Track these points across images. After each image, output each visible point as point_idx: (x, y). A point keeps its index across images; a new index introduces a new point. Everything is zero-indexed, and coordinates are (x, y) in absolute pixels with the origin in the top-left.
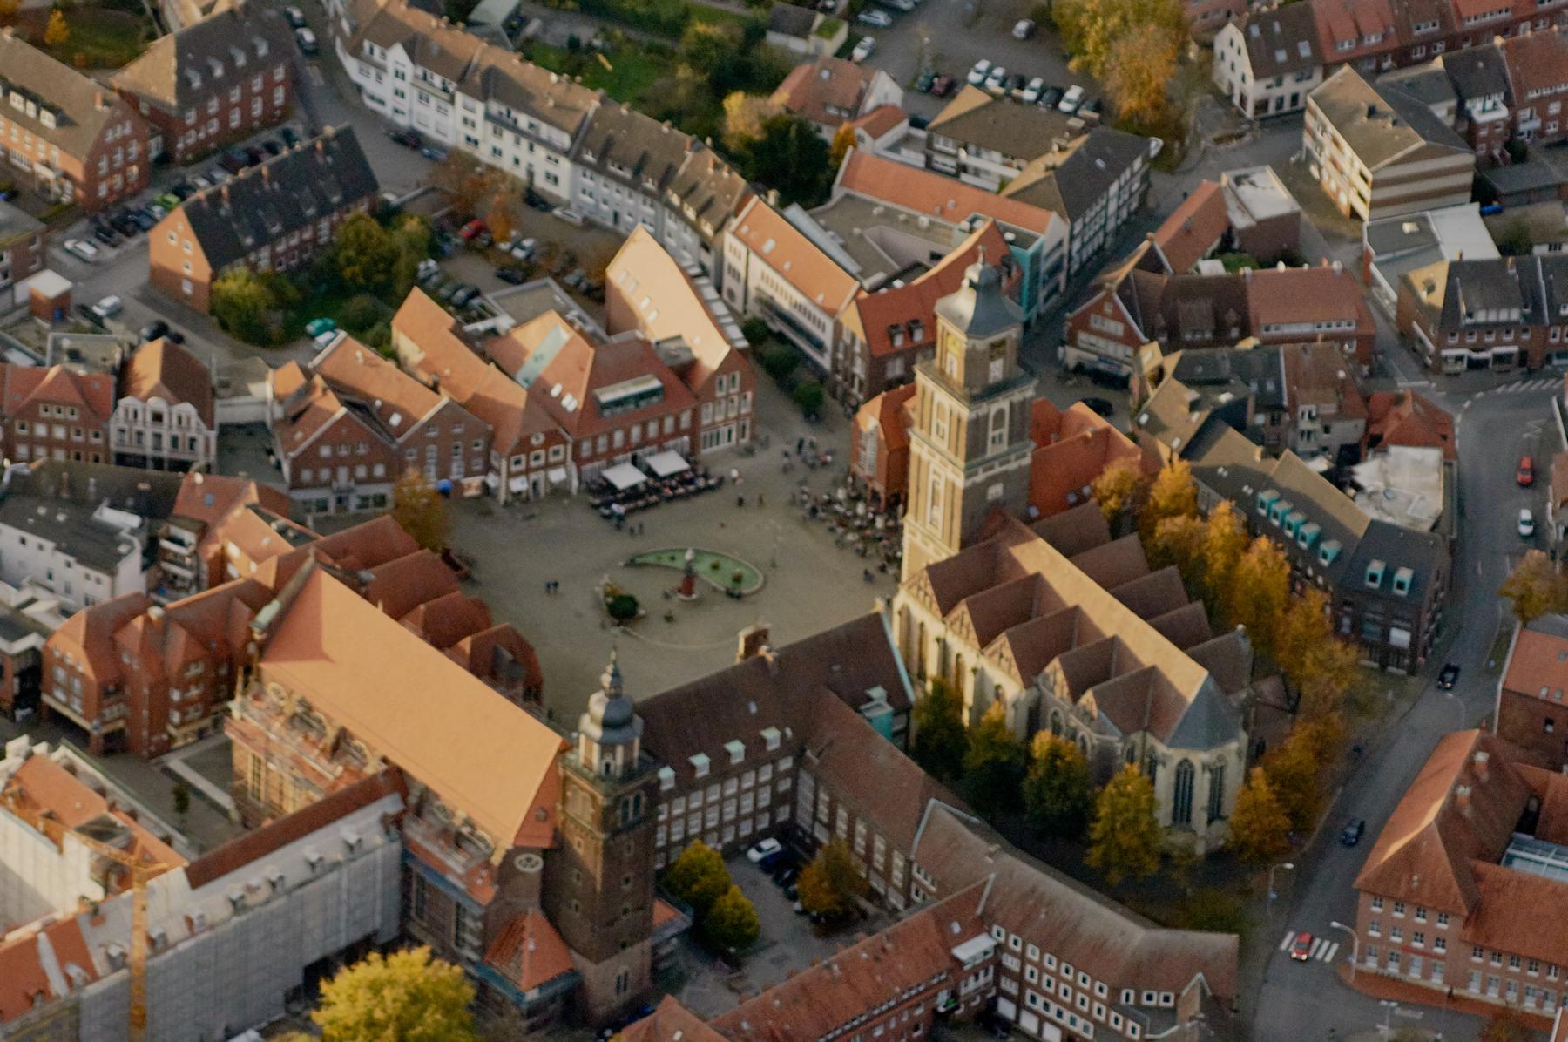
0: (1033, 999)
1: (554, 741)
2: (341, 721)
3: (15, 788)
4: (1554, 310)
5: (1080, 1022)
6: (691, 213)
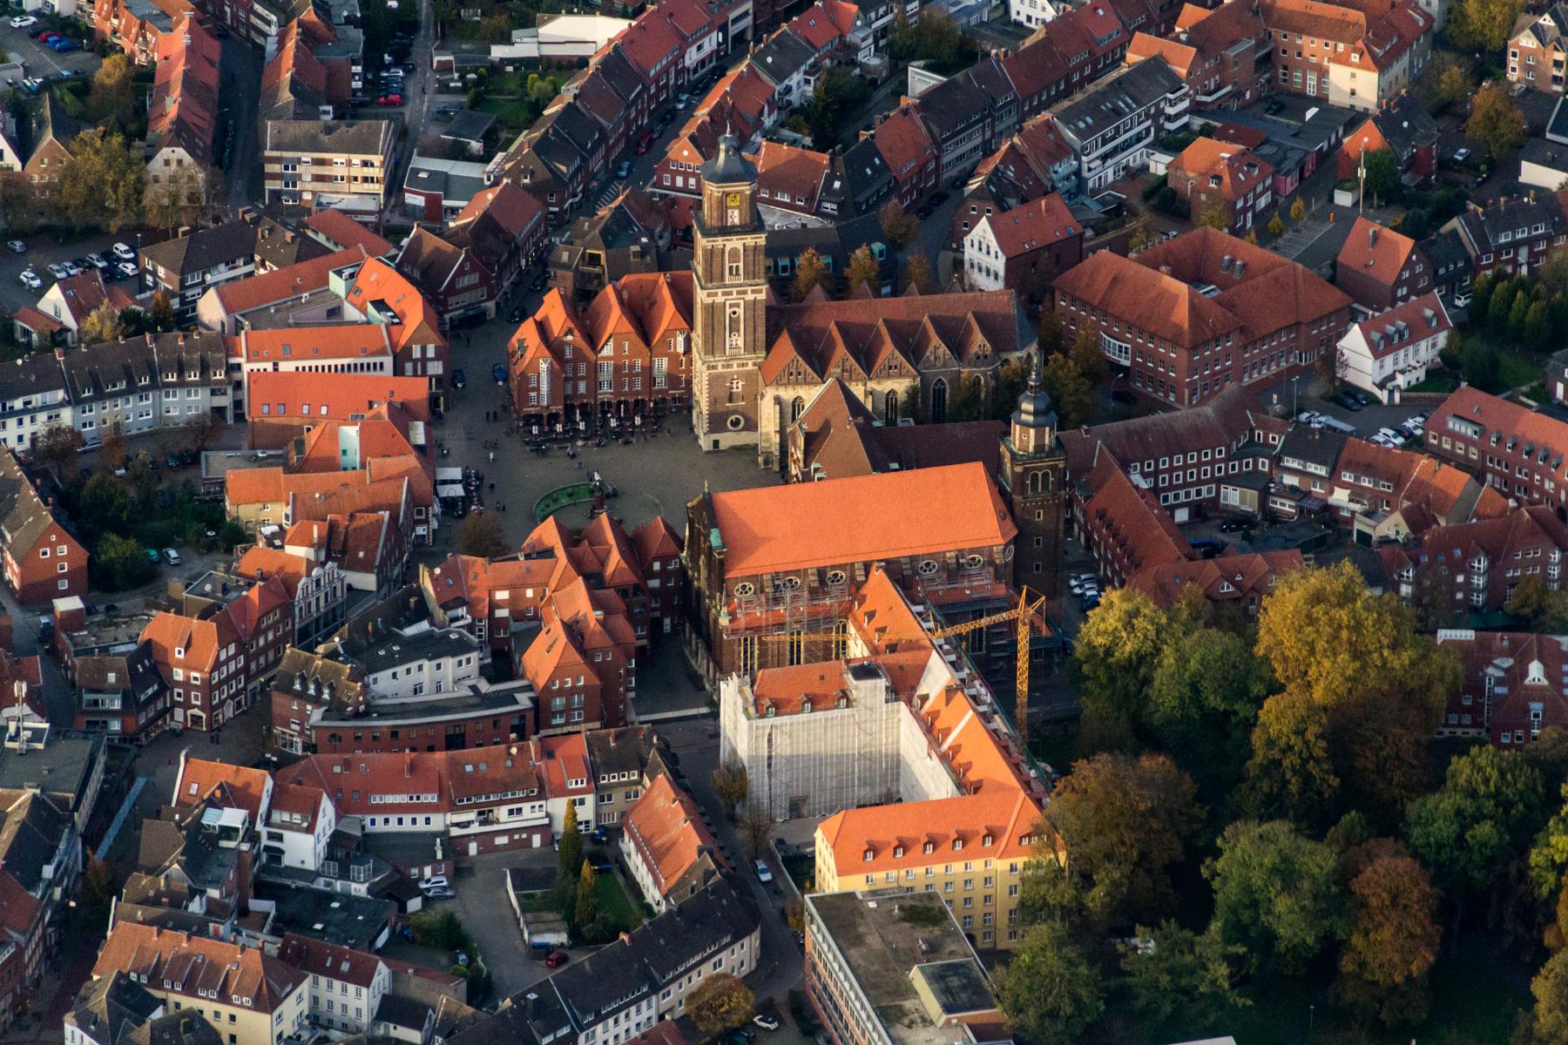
0: (1166, 499)
2: (812, 566)
3: (767, 702)
4: (583, 147)
5: (1204, 489)
6: (193, 377)
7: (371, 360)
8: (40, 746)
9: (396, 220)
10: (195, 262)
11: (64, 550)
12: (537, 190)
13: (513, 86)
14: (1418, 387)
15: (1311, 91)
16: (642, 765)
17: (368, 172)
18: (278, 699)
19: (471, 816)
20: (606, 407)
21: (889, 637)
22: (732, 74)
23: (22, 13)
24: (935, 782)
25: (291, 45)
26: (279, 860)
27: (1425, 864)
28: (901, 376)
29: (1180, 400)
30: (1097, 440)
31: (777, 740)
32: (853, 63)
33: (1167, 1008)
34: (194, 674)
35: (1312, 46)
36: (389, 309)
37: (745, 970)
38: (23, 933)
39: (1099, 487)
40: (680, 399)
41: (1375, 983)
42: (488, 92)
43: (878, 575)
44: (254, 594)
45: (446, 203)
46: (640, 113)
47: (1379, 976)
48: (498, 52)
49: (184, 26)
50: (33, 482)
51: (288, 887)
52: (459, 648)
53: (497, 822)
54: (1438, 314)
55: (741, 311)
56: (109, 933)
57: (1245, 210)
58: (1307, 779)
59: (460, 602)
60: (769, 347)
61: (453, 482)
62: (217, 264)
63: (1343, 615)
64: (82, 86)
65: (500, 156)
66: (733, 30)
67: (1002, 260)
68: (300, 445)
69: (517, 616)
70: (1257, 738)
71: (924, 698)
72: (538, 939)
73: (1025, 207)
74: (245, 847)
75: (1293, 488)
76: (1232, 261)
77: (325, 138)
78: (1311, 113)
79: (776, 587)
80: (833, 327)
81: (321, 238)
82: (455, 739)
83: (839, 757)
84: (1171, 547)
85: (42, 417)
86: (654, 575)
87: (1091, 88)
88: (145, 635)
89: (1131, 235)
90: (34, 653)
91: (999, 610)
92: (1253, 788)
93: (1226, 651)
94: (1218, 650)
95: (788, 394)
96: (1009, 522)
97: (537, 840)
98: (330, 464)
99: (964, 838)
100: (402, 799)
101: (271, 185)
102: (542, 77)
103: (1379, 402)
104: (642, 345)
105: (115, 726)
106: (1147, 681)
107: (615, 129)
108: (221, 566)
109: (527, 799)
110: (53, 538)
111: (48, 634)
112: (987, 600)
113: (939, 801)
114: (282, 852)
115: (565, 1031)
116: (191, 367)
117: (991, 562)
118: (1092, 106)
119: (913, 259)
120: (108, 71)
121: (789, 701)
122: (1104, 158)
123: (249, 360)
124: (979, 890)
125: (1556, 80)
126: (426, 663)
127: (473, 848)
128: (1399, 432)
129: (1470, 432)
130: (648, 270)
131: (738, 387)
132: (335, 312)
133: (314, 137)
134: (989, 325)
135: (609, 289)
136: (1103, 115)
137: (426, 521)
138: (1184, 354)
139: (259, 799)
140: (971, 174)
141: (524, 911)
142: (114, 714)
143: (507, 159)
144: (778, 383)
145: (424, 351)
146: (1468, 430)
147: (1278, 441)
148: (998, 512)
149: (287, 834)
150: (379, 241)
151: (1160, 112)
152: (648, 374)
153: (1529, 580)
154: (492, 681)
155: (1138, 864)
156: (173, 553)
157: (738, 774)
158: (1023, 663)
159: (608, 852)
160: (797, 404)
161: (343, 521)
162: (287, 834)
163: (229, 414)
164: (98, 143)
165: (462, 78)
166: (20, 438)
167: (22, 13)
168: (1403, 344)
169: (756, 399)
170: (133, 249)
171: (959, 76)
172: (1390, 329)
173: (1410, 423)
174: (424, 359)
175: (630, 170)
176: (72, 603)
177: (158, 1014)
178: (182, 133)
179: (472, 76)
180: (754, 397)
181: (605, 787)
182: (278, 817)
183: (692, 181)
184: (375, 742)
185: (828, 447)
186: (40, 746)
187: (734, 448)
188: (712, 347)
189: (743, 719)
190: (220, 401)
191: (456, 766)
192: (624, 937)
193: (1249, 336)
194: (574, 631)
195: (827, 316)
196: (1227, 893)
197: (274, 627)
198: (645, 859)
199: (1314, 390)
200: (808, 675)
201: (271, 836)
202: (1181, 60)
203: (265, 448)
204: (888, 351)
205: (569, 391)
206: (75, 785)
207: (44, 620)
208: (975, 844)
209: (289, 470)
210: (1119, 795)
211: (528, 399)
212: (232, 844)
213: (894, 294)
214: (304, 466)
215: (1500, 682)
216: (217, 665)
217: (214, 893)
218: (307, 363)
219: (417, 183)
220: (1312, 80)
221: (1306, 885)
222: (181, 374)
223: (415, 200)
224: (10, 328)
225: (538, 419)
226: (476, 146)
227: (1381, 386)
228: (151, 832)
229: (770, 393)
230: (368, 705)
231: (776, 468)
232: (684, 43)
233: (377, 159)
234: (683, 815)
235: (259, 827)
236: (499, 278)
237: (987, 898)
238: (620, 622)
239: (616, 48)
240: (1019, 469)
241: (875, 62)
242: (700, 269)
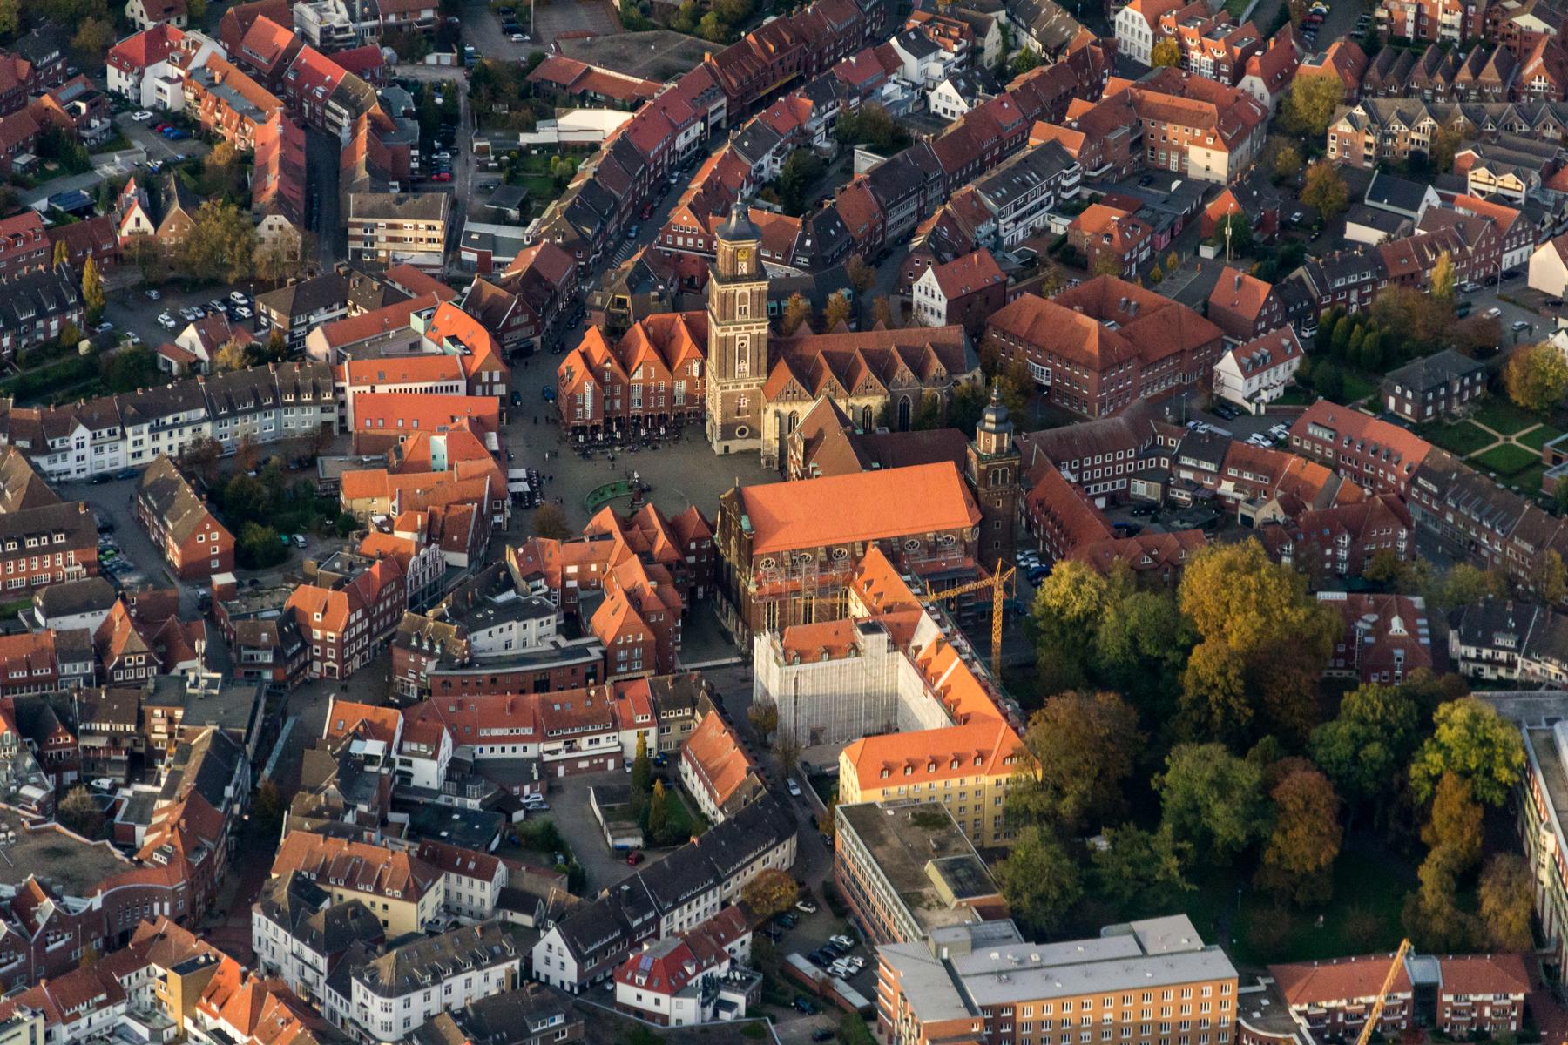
1: (949, 467)
2: (821, 545)
3: (793, 653)
4: (602, 214)
5: (1118, 482)
6: (307, 398)
7: (449, 384)
8: (216, 692)
9: (455, 272)
10: (301, 306)
11: (216, 536)
12: (568, 248)
13: (539, 166)
14: (1278, 401)
15: (1174, 167)
16: (694, 704)
17: (432, 234)
18: (398, 653)
19: (560, 745)
20: (639, 422)
21: (887, 599)
22: (717, 155)
23: (141, 109)
24: (930, 716)
25: (363, 133)
26: (409, 781)
27: (1329, 778)
28: (875, 393)
29: (1091, 412)
30: (1035, 442)
31: (802, 683)
32: (810, 146)
33: (1129, 893)
34: (330, 634)
35: (1174, 131)
36: (461, 343)
37: (786, 865)
38: (213, 841)
39: (1037, 482)
40: (695, 414)
41: (1292, 872)
42: (518, 170)
43: (873, 551)
44: (375, 570)
45: (494, 259)
46: (643, 186)
47: (1294, 866)
48: (525, 139)
49: (276, 119)
50: (189, 482)
51: (417, 803)
52: (540, 612)
53: (580, 749)
54: (1293, 343)
55: (747, 343)
56: (282, 840)
57: (1131, 261)
58: (1228, 710)
59: (538, 575)
60: (769, 372)
61: (519, 480)
62: (317, 308)
63: (1251, 581)
64: (195, 168)
65: (535, 221)
66: (712, 121)
67: (944, 302)
68: (399, 451)
69: (584, 586)
70: (1188, 678)
71: (918, 649)
72: (619, 843)
73: (958, 263)
74: (385, 771)
75: (1188, 481)
76: (1128, 302)
77: (397, 208)
78: (1175, 185)
79: (792, 562)
80: (819, 355)
81: (398, 286)
82: (542, 685)
83: (851, 697)
84: (1100, 528)
85: (188, 431)
86: (690, 553)
87: (1004, 165)
88: (288, 604)
89: (1044, 282)
90: (194, 618)
91: (967, 580)
92: (1184, 719)
93: (1159, 610)
94: (1152, 609)
95: (786, 409)
96: (975, 508)
97: (611, 764)
98: (424, 467)
99: (959, 759)
100: (505, 732)
101: (353, 245)
102: (563, 158)
103: (1249, 413)
104: (665, 369)
105: (268, 675)
106: (1092, 634)
107: (626, 196)
108: (347, 548)
109: (603, 731)
110: (208, 526)
111: (206, 605)
112: (957, 570)
113: (932, 732)
114: (411, 775)
115: (651, 915)
116: (306, 390)
117: (962, 541)
118: (1005, 179)
119: (879, 303)
120: (218, 156)
121: (810, 652)
122: (1016, 220)
123: (351, 384)
124: (971, 801)
125: (1367, 158)
126: (515, 624)
127: (561, 771)
128: (1267, 437)
129: (1326, 436)
130: (665, 311)
131: (745, 403)
132: (416, 346)
133: (388, 206)
134: (943, 353)
135: (638, 327)
136: (1014, 186)
137: (502, 511)
138: (1095, 375)
139: (393, 733)
140: (912, 233)
141: (607, 819)
142: (267, 666)
143: (543, 223)
144: (778, 400)
145: (491, 376)
146: (1324, 435)
147: (1175, 444)
148: (967, 501)
149: (416, 761)
150: (445, 288)
151: (1058, 184)
152: (670, 394)
153: (1382, 552)
154: (568, 638)
155: (1096, 779)
156: (300, 538)
157: (770, 710)
158: (997, 621)
159: (670, 773)
160: (793, 418)
161: (440, 511)
162: (416, 761)
163: (335, 428)
164: (218, 212)
165: (497, 159)
166: (170, 448)
167: (141, 109)
168: (1266, 367)
169: (759, 412)
170: (246, 296)
171: (898, 156)
172: (1256, 355)
173: (1275, 430)
174: (491, 383)
175: (637, 232)
176: (224, 579)
177: (326, 904)
178: (282, 204)
179: (505, 158)
180: (757, 412)
181: (665, 721)
182: (407, 747)
183: (690, 241)
184: (478, 687)
185: (822, 450)
186: (216, 692)
187: (743, 453)
188: (724, 371)
189: (774, 667)
190: (328, 417)
191: (546, 705)
192: (694, 840)
193: (1145, 362)
194: (634, 597)
195: (814, 347)
196: (1173, 801)
197: (391, 595)
198: (701, 777)
199: (1197, 404)
200: (821, 632)
201: (403, 762)
202: (1074, 143)
203: (368, 454)
204: (865, 374)
205: (607, 407)
206: (246, 724)
207: (202, 592)
208: (968, 763)
209: (392, 471)
210: (1083, 724)
211: (576, 414)
212: (374, 769)
213: (858, 329)
214: (403, 468)
215: (1368, 633)
216: (348, 627)
217: (363, 808)
218: (397, 387)
219: (470, 242)
220: (1174, 159)
221: (1237, 794)
222: (297, 395)
223: (470, 256)
224: (155, 360)
225: (583, 430)
226: (514, 213)
227: (1250, 400)
228: (311, 759)
229: (772, 408)
230: (471, 657)
231: (776, 467)
232: (676, 131)
233: (439, 224)
234: (732, 743)
235: (394, 755)
236: (544, 318)
237: (976, 807)
238: (670, 590)
239: (623, 135)
240: (983, 467)
241: (826, 145)
242: (715, 310)
